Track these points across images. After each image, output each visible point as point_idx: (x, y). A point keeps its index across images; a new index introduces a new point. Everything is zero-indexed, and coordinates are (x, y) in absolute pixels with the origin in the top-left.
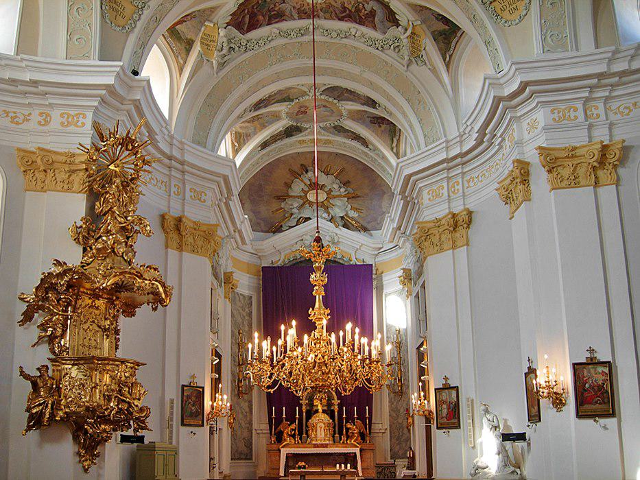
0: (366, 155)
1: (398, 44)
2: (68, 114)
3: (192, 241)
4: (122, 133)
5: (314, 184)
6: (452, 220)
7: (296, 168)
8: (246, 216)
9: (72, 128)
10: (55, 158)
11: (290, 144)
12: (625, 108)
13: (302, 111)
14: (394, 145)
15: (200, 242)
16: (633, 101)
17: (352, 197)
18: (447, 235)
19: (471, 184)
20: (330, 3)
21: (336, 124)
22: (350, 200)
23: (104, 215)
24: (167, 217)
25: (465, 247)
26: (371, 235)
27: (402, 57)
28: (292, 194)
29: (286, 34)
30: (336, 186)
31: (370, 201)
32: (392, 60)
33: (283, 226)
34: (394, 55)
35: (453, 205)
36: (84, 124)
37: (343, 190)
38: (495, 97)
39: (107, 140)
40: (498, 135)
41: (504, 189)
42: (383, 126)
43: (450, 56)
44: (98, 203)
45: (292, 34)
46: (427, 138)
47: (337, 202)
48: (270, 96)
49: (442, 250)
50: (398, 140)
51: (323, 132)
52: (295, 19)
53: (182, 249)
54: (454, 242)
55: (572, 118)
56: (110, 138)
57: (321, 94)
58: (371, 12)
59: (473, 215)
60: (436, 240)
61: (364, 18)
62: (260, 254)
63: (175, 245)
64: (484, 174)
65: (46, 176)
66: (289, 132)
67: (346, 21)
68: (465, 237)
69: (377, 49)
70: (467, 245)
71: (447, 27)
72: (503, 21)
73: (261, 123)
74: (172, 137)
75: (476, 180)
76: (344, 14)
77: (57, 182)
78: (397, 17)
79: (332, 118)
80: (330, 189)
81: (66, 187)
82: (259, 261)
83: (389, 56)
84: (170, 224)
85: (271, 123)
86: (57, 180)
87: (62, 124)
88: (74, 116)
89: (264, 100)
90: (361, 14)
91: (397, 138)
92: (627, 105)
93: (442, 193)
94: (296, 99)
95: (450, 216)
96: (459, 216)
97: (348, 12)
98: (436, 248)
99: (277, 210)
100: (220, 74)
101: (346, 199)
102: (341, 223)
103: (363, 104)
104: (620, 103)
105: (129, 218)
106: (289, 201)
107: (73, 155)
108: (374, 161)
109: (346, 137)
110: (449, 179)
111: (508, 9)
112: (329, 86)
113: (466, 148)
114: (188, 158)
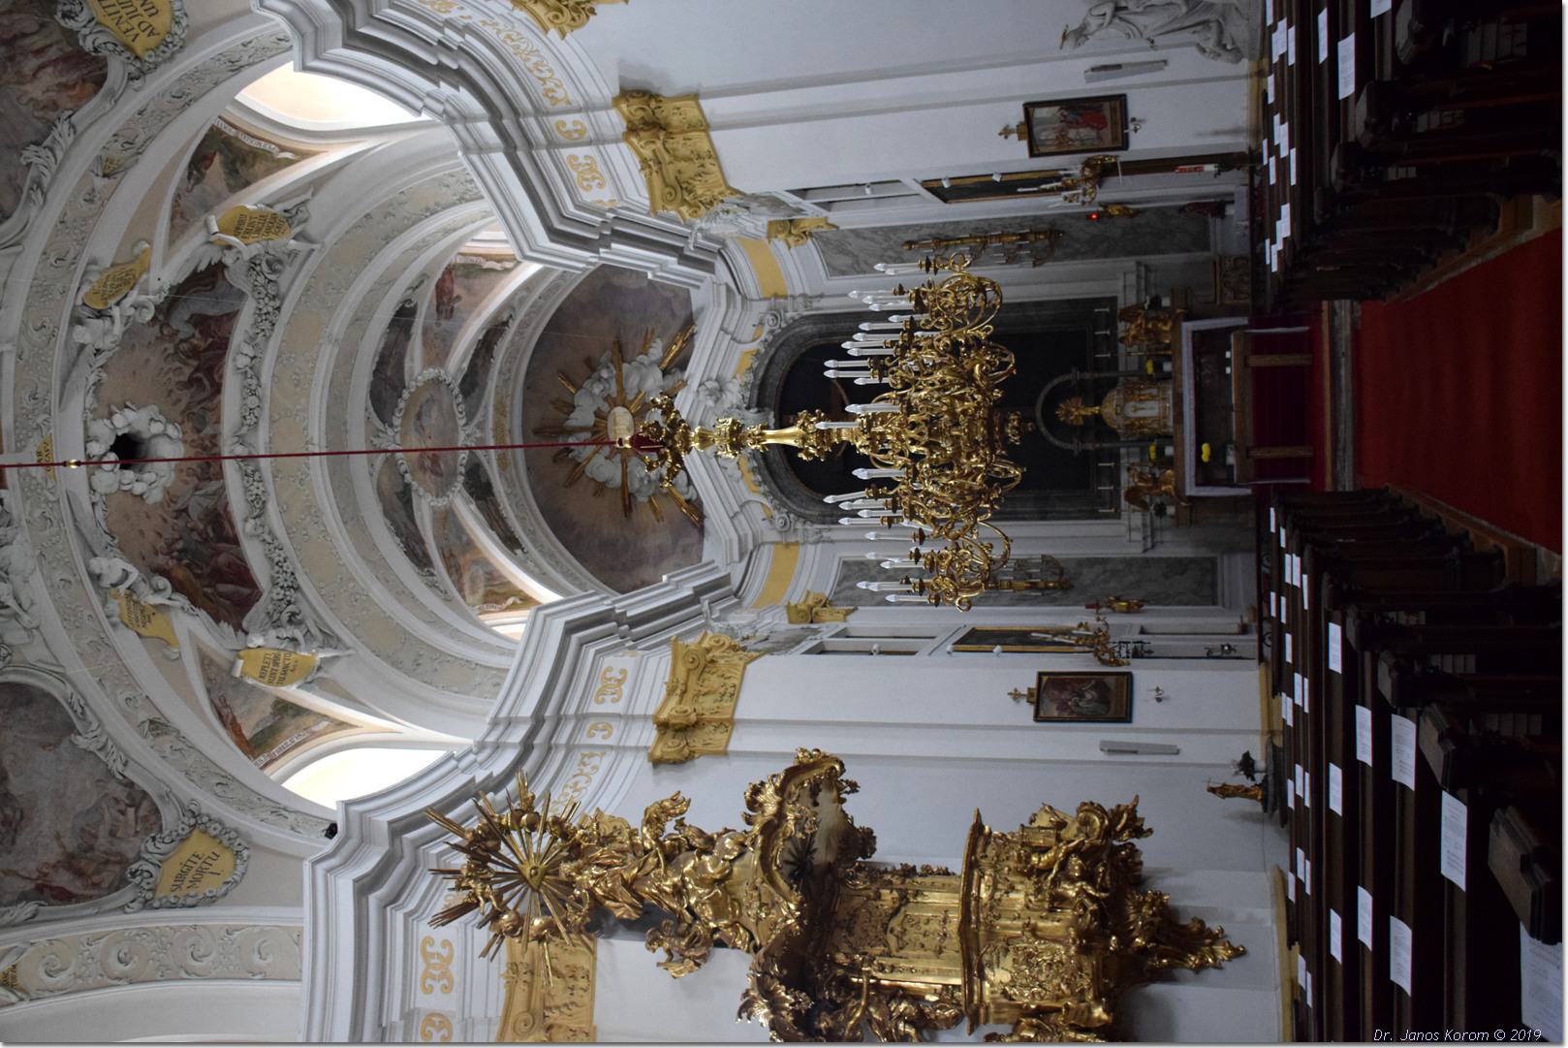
0: (524, 325)
1: (265, 267)
2: (427, 975)
3: (710, 699)
4: (461, 861)
5: (593, 434)
6: (642, 134)
7: (562, 472)
8: (665, 578)
9: (455, 968)
10: (519, 1005)
11: (509, 487)
13: (433, 461)
14: (498, 266)
15: (713, 681)
17: (621, 353)
18: (678, 143)
19: (560, 94)
20: (183, 412)
21: (457, 391)
23: (641, 899)
24: (658, 753)
25: (703, 103)
26: (702, 309)
27: (293, 254)
28: (618, 480)
29: (258, 507)
30: (597, 390)
32: (302, 274)
33: (688, 497)
34: (288, 272)
35: (608, 132)
36: (446, 943)
37: (605, 374)
38: (346, 46)
39: (474, 895)
40: (438, 35)
41: (557, 17)
42: (457, 290)
43: (283, 149)
44: (618, 913)
45: (255, 491)
46: (467, 197)
47: (632, 382)
48: (398, 533)
49: (713, 155)
50: (488, 257)
51: (478, 418)
52: (223, 488)
53: (728, 720)
54: (692, 127)
56: (469, 888)
57: (391, 425)
58: (195, 326)
59: (629, 87)
60: (689, 169)
61: (210, 340)
62: (750, 547)
63: (719, 737)
64: (536, 64)
65: (560, 1026)
66: (480, 489)
67: (221, 377)
68: (678, 104)
69: (278, 309)
70: (695, 97)
71: (217, 159)
72: (176, 29)
73: (458, 554)
74: (481, 746)
75: (550, 85)
76: (206, 382)
77: (573, 1003)
78: (202, 267)
79: (446, 399)
81: (582, 983)
82: (767, 546)
83: (294, 284)
84: (671, 747)
85: (460, 530)
86: (567, 1001)
87: (447, 989)
88: (429, 965)
89: (407, 545)
90: (203, 345)
91: (482, 260)
93: (586, 157)
94: (403, 477)
95: (634, 140)
96: (632, 118)
97: (200, 375)
98: (709, 167)
99: (655, 510)
100: (349, 643)
101: (625, 366)
102: (678, 375)
103: (408, 336)
105: (647, 845)
106: (634, 485)
107: (513, 967)
108: (536, 308)
109: (487, 371)
110: (552, 145)
112: (371, 409)
113: (475, 106)
114: (527, 709)
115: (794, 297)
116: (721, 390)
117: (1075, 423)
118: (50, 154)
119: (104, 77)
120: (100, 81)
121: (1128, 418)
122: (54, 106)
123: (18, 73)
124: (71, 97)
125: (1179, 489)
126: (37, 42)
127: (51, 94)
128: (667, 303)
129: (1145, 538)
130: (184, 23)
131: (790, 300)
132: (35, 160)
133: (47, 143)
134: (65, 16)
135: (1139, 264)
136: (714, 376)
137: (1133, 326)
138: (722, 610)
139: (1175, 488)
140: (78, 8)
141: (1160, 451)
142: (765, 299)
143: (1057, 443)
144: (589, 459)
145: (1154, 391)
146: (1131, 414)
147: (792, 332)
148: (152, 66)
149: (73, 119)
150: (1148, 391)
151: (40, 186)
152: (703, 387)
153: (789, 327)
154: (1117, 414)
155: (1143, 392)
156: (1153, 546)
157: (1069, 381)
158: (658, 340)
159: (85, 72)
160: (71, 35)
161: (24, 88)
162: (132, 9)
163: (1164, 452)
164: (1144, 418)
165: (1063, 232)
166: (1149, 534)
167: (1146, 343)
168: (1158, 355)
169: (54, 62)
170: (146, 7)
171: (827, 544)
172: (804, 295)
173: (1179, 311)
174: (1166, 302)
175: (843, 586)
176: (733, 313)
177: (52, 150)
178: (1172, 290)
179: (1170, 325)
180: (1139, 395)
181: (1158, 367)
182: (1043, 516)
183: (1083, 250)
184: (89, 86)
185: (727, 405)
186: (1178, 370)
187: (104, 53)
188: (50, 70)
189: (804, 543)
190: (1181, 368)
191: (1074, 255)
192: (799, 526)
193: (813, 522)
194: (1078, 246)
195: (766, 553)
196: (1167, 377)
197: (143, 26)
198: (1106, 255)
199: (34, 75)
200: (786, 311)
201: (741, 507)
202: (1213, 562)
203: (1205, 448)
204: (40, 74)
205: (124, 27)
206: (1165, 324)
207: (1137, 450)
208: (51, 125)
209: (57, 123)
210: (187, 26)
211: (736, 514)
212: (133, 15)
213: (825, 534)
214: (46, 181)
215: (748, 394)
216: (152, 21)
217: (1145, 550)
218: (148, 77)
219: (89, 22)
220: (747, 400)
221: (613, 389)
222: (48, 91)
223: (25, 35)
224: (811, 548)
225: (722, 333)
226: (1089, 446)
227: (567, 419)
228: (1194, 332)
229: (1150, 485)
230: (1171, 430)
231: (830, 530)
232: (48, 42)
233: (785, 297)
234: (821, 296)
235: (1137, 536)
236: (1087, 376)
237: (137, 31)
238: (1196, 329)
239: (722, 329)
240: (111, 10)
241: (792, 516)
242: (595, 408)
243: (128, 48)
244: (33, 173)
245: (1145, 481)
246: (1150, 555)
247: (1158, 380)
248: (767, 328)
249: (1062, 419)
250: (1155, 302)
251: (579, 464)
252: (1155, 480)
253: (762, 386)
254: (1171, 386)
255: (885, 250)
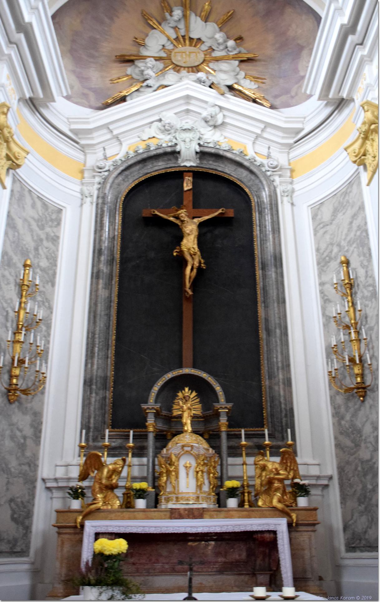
5: (183, 37)
22: (244, 65)
28: (144, 53)
31: (277, 66)
47: (224, 66)
62: (82, 142)
80: (210, 48)
101: (237, 63)
106: (140, 64)
115: (291, 183)
116: (215, 127)
117: (175, 407)
121: (178, 457)
125: (89, 514)
128: (287, 91)
129: (56, 480)
131: (289, 180)
135: (331, 478)
136: (227, 120)
137: (277, 466)
138: (10, 56)
139: (98, 509)
141: (141, 494)
142: (289, 164)
143: (156, 388)
144: (163, 32)
145: (206, 488)
146: (183, 462)
147: (262, 179)
150: (206, 482)
152: (217, 109)
153: (267, 178)
154: (183, 446)
155: (205, 475)
156: (48, 489)
157: (218, 401)
158: (256, 86)
163: (140, 497)
164: (177, 477)
165: (363, 401)
166: (61, 484)
167: (258, 482)
168: (243, 493)
171: (79, 202)
172: (293, 191)
173: (294, 516)
174: (302, 502)
175: (37, 200)
176: (278, 136)
178: (315, 509)
179: (280, 506)
180: (202, 472)
181: (232, 492)
182: (88, 383)
183: (343, 422)
185: (203, 131)
186: (229, 514)
189: (82, 184)
190: (231, 517)
191: (337, 415)
192: (97, 179)
193: (99, 189)
194: (348, 417)
195: (78, 155)
196: (220, 503)
198: (338, 445)
200: (280, 176)
201: (117, 138)
202: (23, 553)
203: (121, 545)
206: (279, 501)
207: (145, 475)
211: (111, 132)
213: (88, 200)
215: (211, 145)
217: (44, 480)
220: (206, 145)
221: (216, 54)
224: (78, 188)
225: (262, 126)
226: (150, 420)
227: (196, 15)
228: (275, 532)
229: (104, 481)
230: (163, 507)
231: (92, 203)
233: (291, 177)
234: (292, 204)
235: (60, 473)
236: (223, 420)
238: (279, 536)
239: (267, 125)
241: (106, 173)
242: (204, 39)
245: (109, 477)
246: (39, 485)
247: (218, 494)
248: (265, 162)
249: (180, 394)
250: (303, 490)
251: (160, 24)
252: (112, 488)
253: (218, 157)
254: (212, 506)
255: (339, 245)
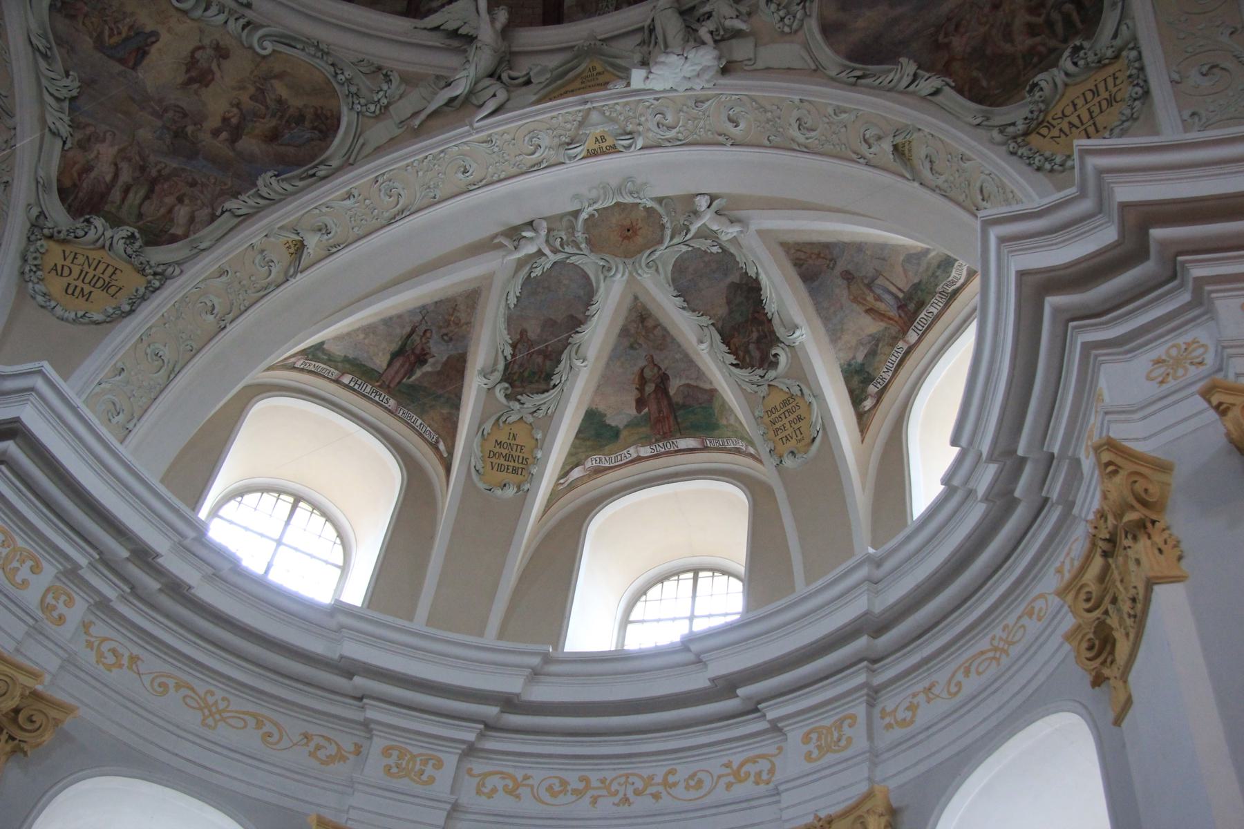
12: (114, 651)
16: (136, 651)
55: (18, 579)
92: (121, 650)
104: (113, 634)
111: (70, 279)
118: (56, 94)
119: (63, 200)
120: (63, 193)
122: (83, 145)
123: (130, 160)
124: (75, 163)
126: (135, 198)
127: (92, 156)
130: (40, 299)
132: (67, 82)
133: (66, 104)
134: (132, 236)
140: (129, 251)
148: (33, 238)
149: (59, 143)
151: (45, 56)
159: (81, 194)
160: (115, 222)
161: (116, 148)
162: (87, 280)
169: (110, 187)
170: (78, 290)
177: (58, 99)
184: (67, 183)
187: (79, 223)
188: (108, 178)
197: (66, 271)
199: (116, 165)
204: (112, 169)
205: (81, 259)
208: (75, 125)
209: (70, 129)
210: (34, 298)
212: (82, 275)
214: (43, 64)
216: (65, 281)
218: (28, 225)
219: (111, 244)
222: (97, 157)
223: (147, 197)
232: (127, 203)
237: (68, 263)
240: (102, 267)
243: (64, 241)
244: (59, 66)
